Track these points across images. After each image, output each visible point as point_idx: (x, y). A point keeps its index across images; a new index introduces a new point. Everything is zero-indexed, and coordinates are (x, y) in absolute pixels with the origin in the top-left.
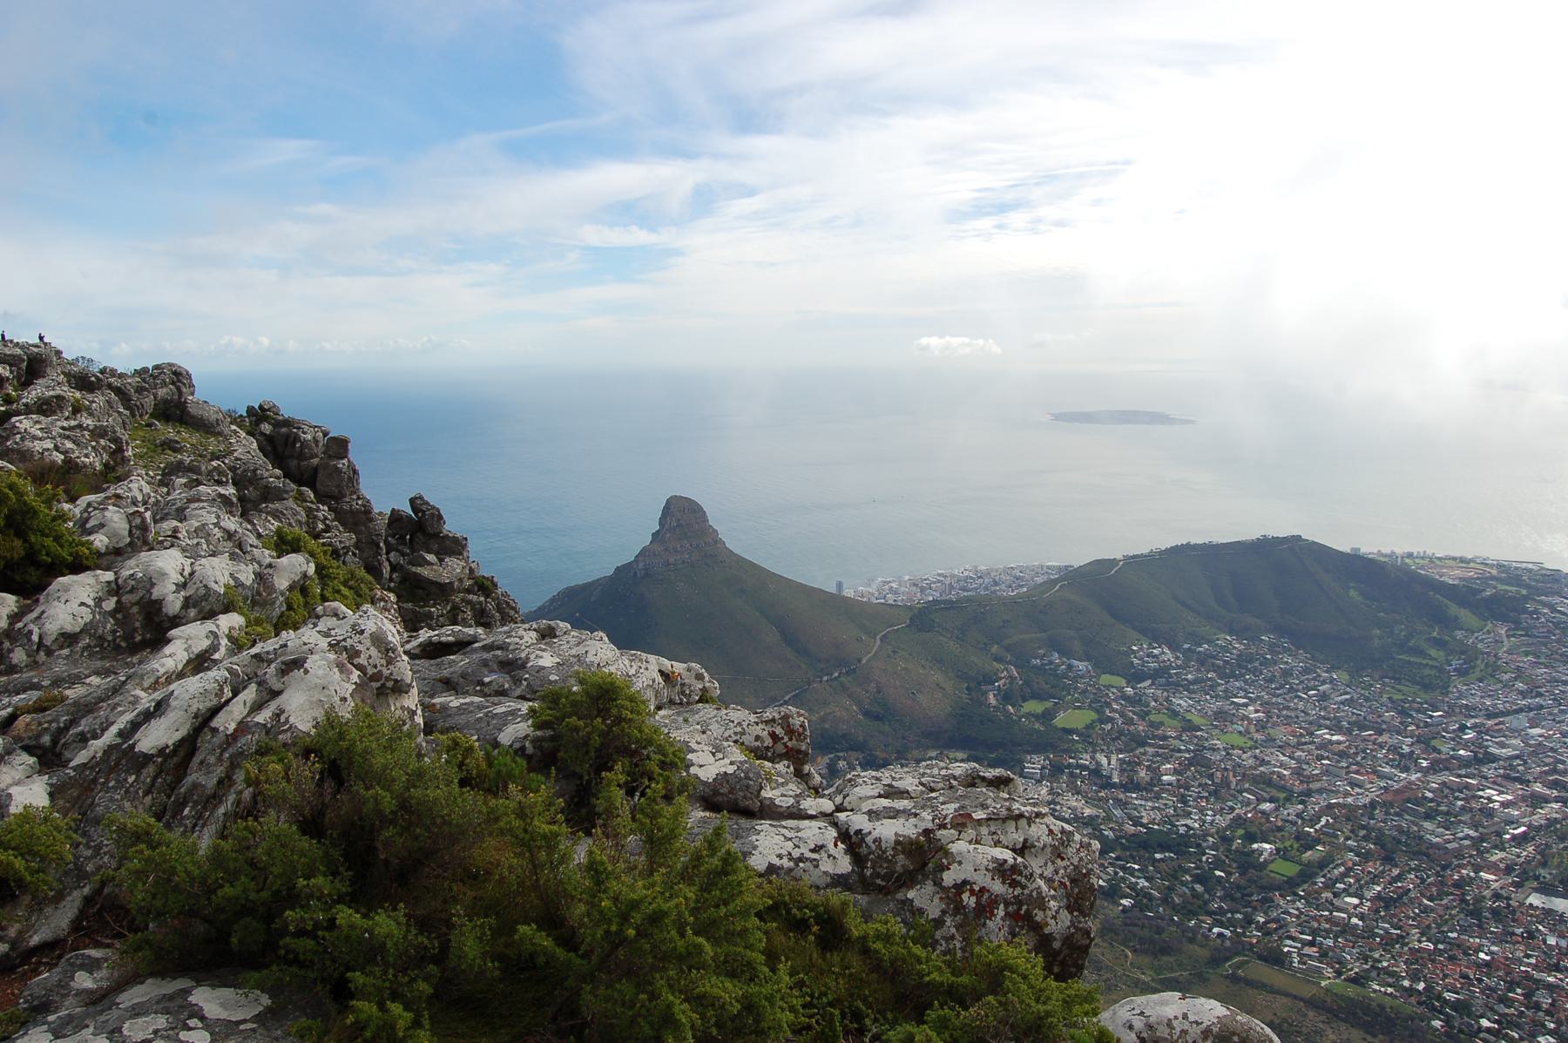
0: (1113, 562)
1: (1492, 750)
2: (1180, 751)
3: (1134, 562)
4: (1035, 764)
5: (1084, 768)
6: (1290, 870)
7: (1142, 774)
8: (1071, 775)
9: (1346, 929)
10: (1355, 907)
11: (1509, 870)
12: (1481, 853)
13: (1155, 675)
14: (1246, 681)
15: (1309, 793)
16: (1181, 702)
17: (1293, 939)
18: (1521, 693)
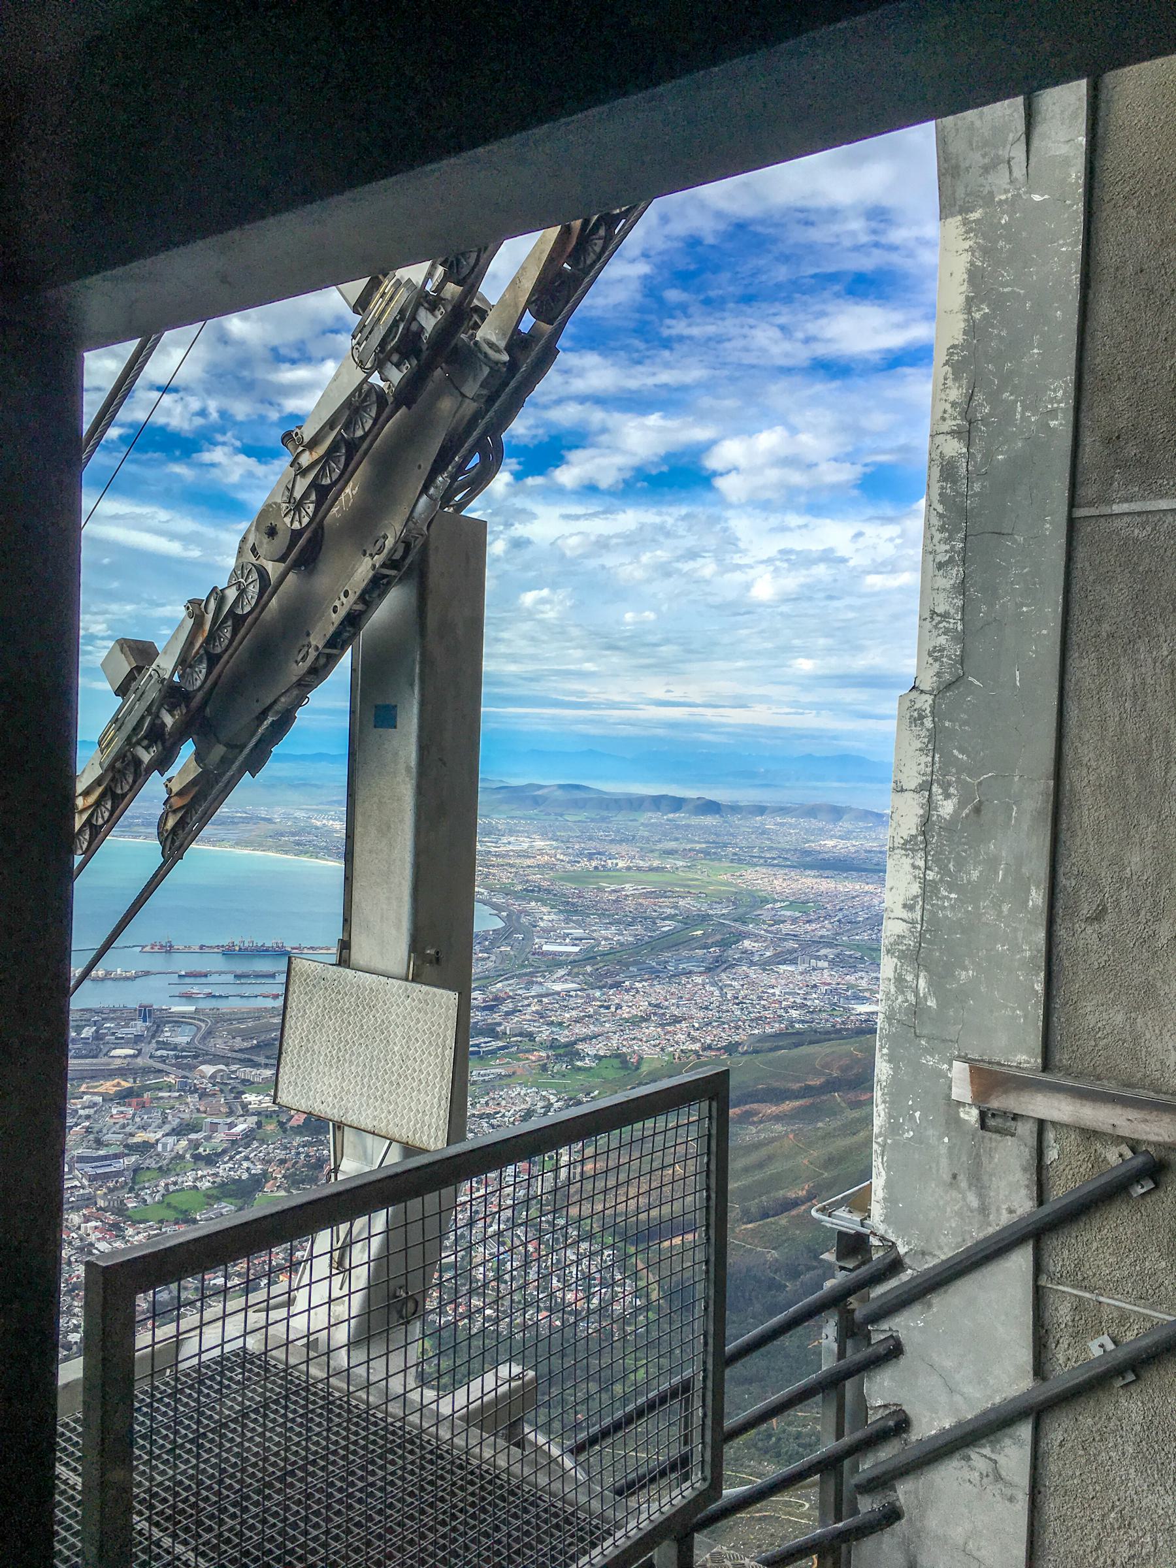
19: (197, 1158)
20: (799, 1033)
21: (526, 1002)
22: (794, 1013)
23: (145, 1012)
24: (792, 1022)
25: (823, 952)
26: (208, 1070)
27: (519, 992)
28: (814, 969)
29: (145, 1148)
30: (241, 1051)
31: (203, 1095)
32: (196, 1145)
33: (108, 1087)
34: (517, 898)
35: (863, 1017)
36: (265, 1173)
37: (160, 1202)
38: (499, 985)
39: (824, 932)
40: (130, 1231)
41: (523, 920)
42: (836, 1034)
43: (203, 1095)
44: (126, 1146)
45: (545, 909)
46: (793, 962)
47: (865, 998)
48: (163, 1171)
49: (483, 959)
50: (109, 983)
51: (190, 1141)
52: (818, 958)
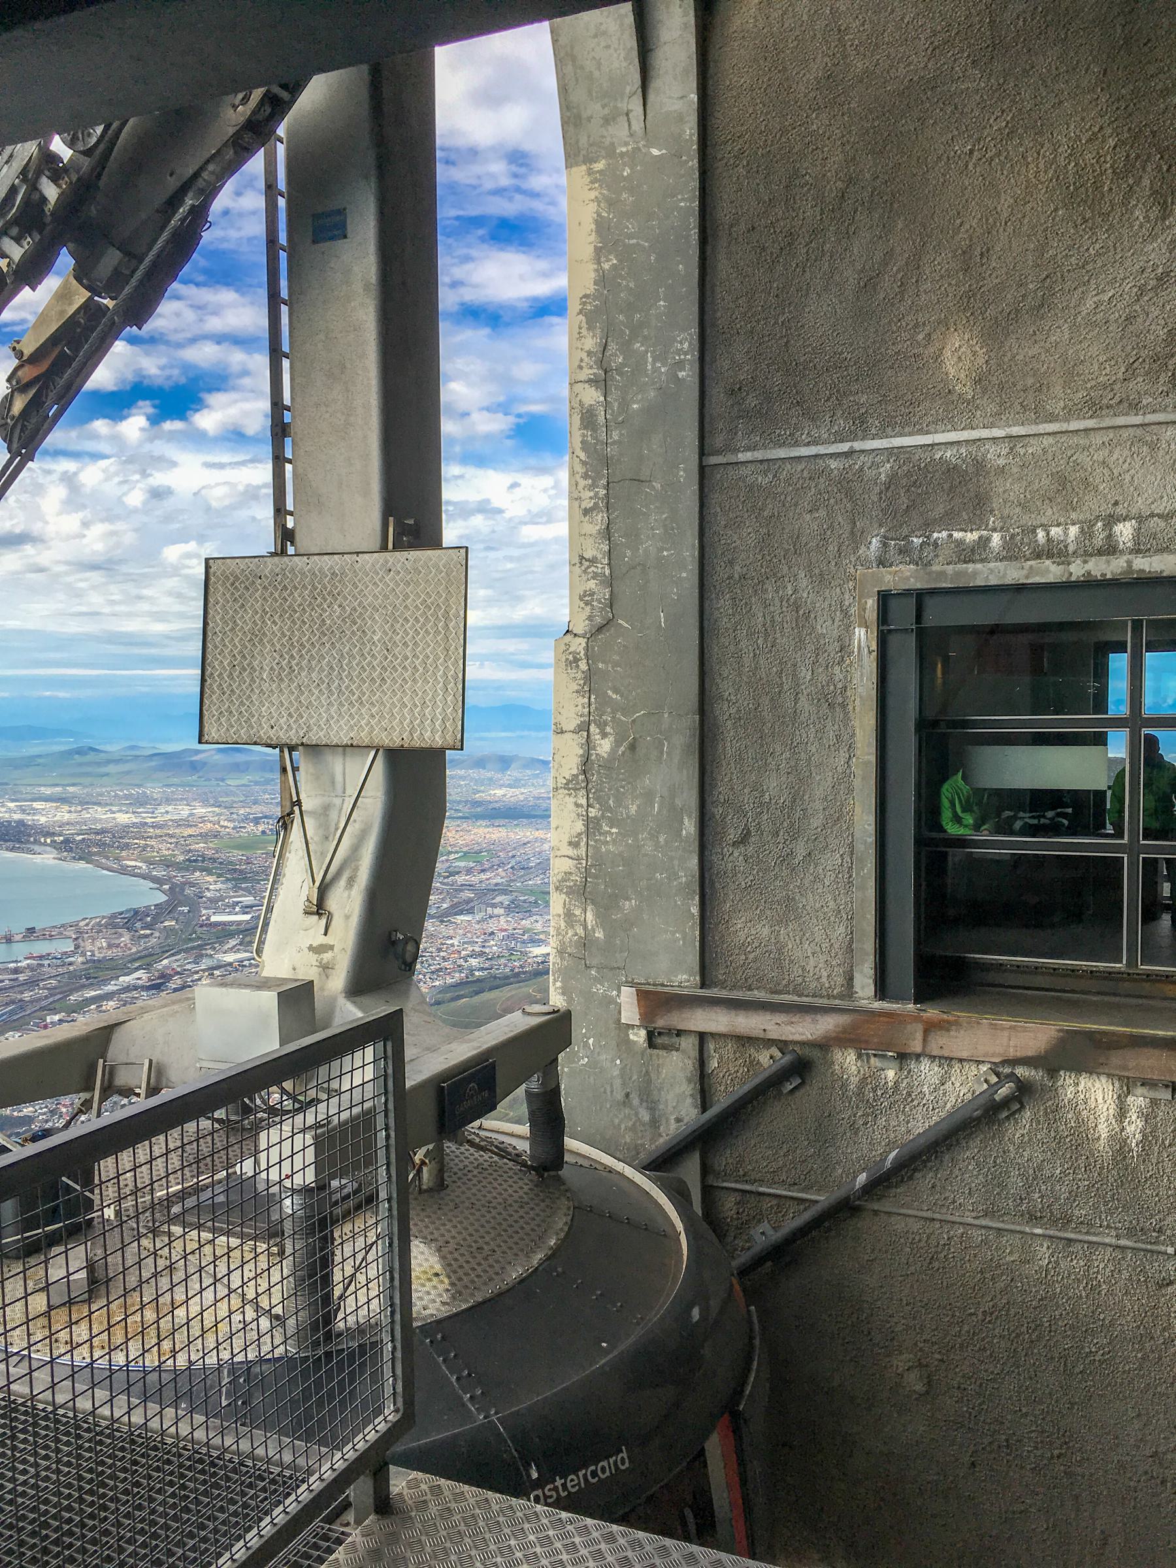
20: (479, 980)
21: (196, 977)
22: (474, 962)
24: (471, 971)
25: (498, 899)
27: (188, 967)
28: (491, 917)
34: (180, 869)
35: (540, 959)
38: (165, 962)
39: (498, 880)
41: (187, 892)
42: (515, 978)
45: (210, 879)
46: (470, 911)
47: (543, 941)
49: (146, 936)
52: (494, 906)
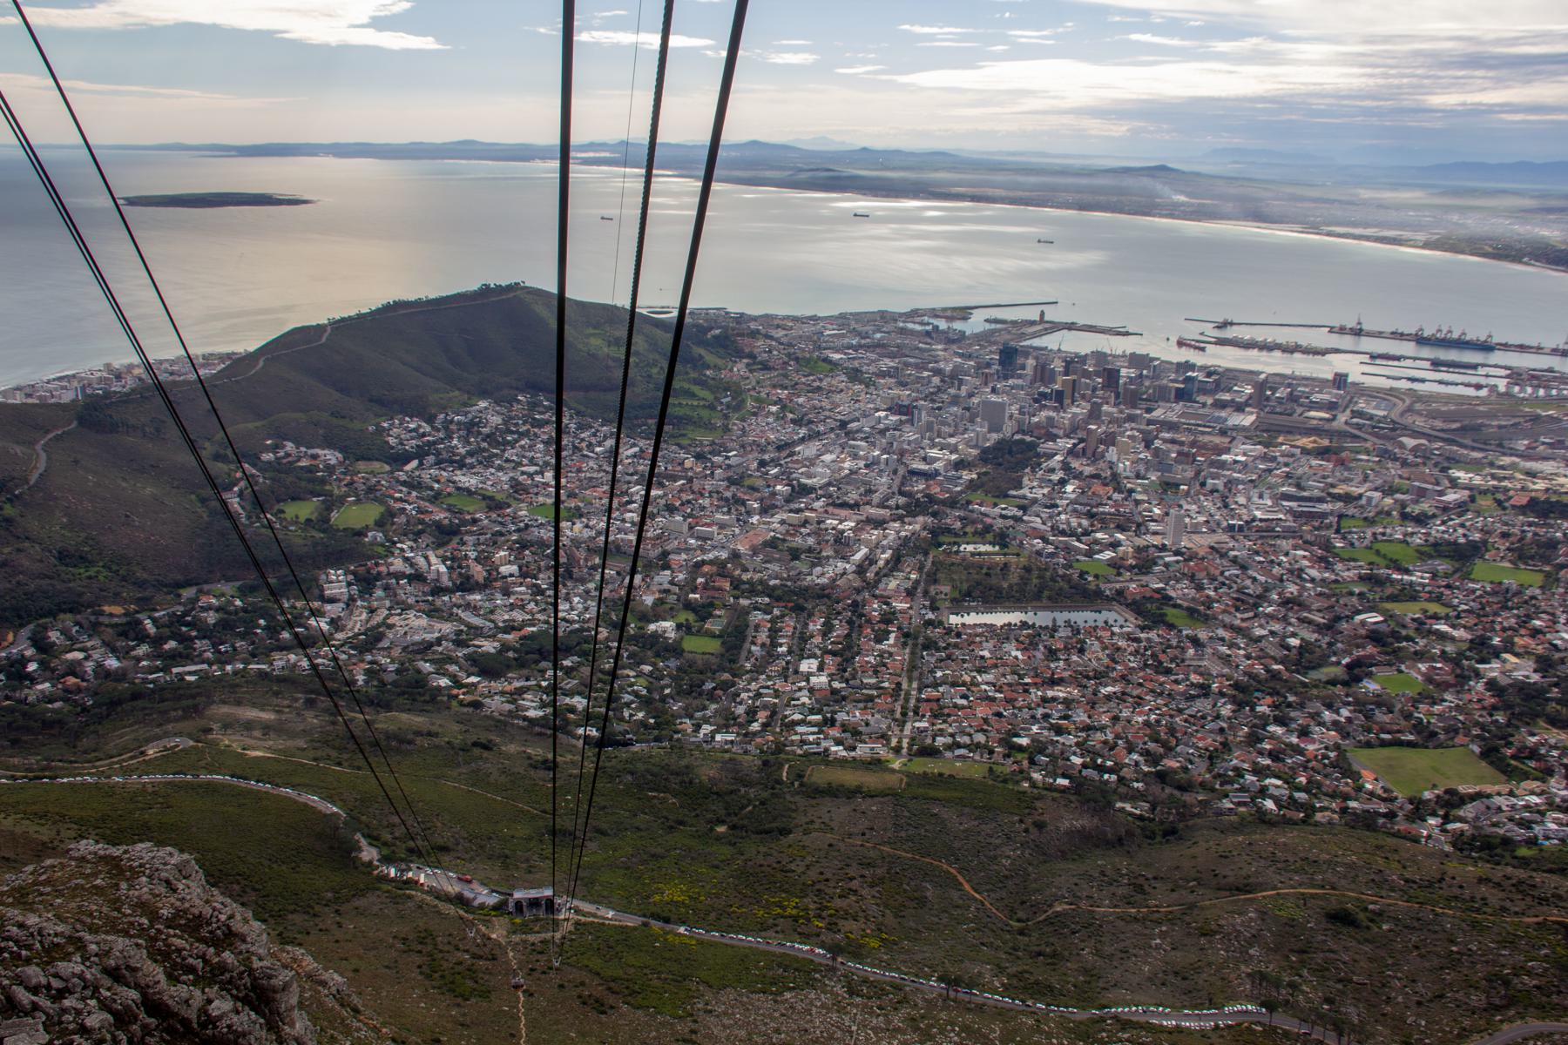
0: (319, 328)
1: (804, 481)
2: (502, 534)
3: (344, 327)
4: (336, 582)
5: (399, 576)
6: (714, 646)
7: (479, 568)
8: (386, 588)
9: (836, 697)
10: (821, 668)
11: (910, 593)
12: (871, 586)
13: (420, 454)
14: (522, 447)
15: (665, 554)
16: (467, 480)
17: (799, 723)
18: (793, 421)
19: (1405, 517)
23: (1340, 380)
26: (1410, 442)
29: (1348, 498)
30: (1442, 430)
31: (1404, 463)
32: (1403, 505)
33: (1305, 442)
36: (1485, 542)
37: (1367, 547)
40: (1339, 567)
43: (1404, 463)
44: (1329, 494)
48: (1370, 522)
50: (1297, 355)
51: (1396, 501)
